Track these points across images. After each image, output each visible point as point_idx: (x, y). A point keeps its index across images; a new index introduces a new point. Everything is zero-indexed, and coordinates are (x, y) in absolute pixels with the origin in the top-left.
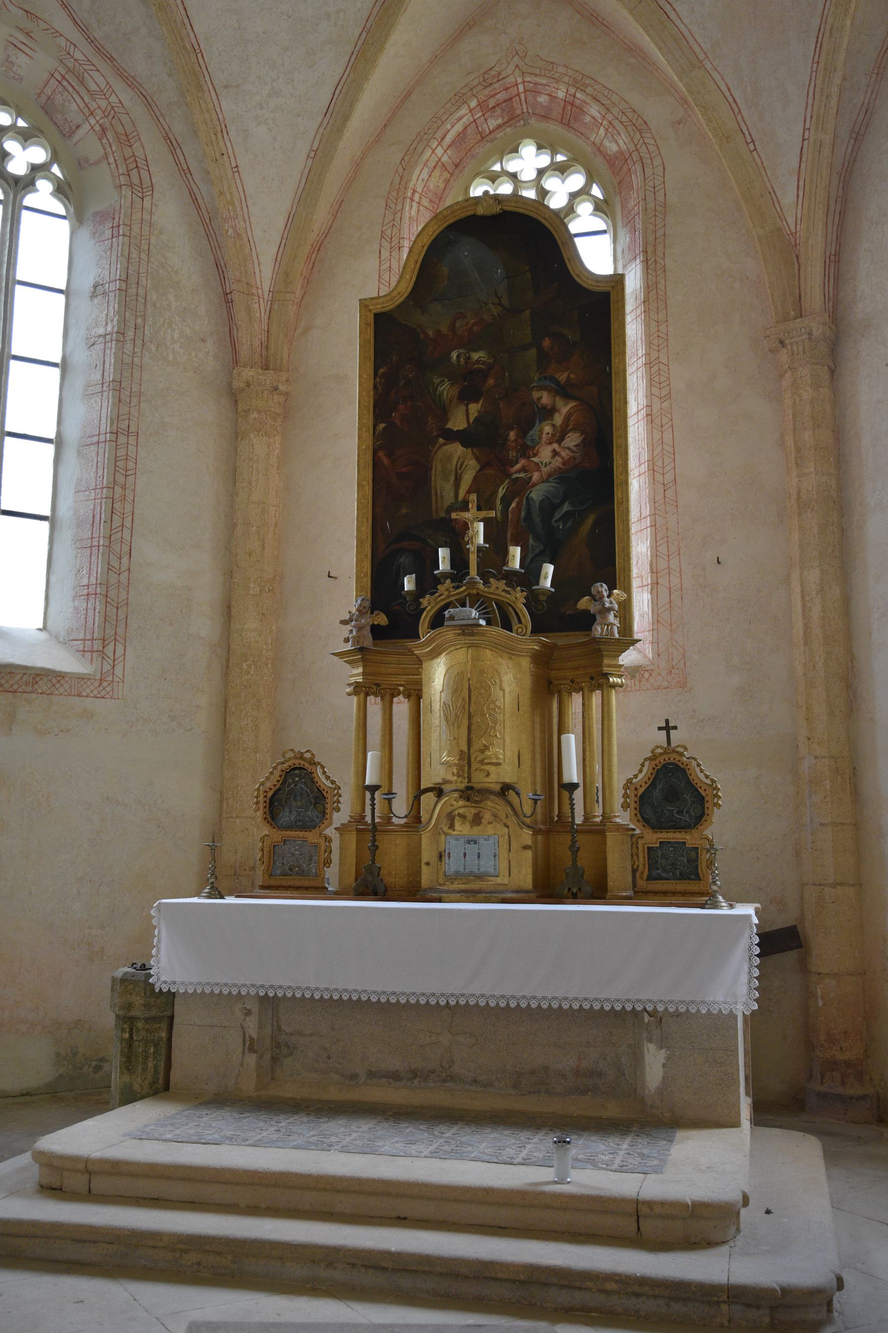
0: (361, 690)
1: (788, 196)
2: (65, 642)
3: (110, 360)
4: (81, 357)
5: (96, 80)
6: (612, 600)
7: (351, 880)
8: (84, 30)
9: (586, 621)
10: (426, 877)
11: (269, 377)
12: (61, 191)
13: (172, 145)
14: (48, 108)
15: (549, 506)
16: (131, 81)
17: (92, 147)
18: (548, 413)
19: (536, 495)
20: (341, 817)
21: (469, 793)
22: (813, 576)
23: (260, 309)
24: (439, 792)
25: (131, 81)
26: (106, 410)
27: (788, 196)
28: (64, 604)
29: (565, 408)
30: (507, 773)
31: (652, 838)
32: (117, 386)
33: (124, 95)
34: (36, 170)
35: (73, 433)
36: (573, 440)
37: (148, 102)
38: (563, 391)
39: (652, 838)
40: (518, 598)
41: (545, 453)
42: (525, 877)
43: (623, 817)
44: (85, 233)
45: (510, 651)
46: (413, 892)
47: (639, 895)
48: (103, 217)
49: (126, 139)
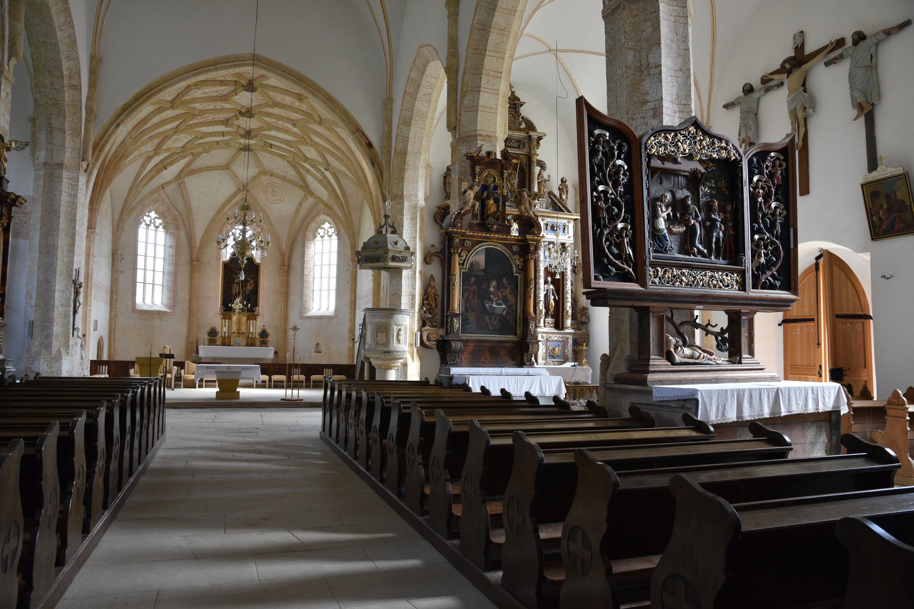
0: (222, 319)
1: (284, 247)
2: (166, 306)
3: (174, 260)
4: (167, 258)
5: (172, 211)
6: (257, 309)
7: (221, 343)
8: (171, 202)
9: (254, 311)
10: (232, 343)
11: (198, 263)
12: (164, 228)
13: (183, 221)
14: (163, 214)
15: (249, 295)
16: (177, 210)
17: (170, 222)
18: (249, 281)
19: (247, 293)
20: (219, 336)
21: (239, 333)
22: (283, 304)
23: (197, 250)
24: (234, 333)
25: (177, 210)
26: (173, 268)
27: (284, 247)
28: (165, 301)
29: (252, 281)
30: (243, 331)
31: (261, 339)
32: (175, 264)
33: (176, 213)
34: (160, 224)
35: (166, 271)
36: (253, 286)
37: (179, 213)
38: (252, 279)
39: (261, 339)
40: (246, 308)
41: (249, 287)
42: (245, 344)
43: (257, 337)
44: (168, 235)
45: (245, 315)
46: (229, 345)
47: (259, 346)
48: (171, 234)
49: (176, 220)
